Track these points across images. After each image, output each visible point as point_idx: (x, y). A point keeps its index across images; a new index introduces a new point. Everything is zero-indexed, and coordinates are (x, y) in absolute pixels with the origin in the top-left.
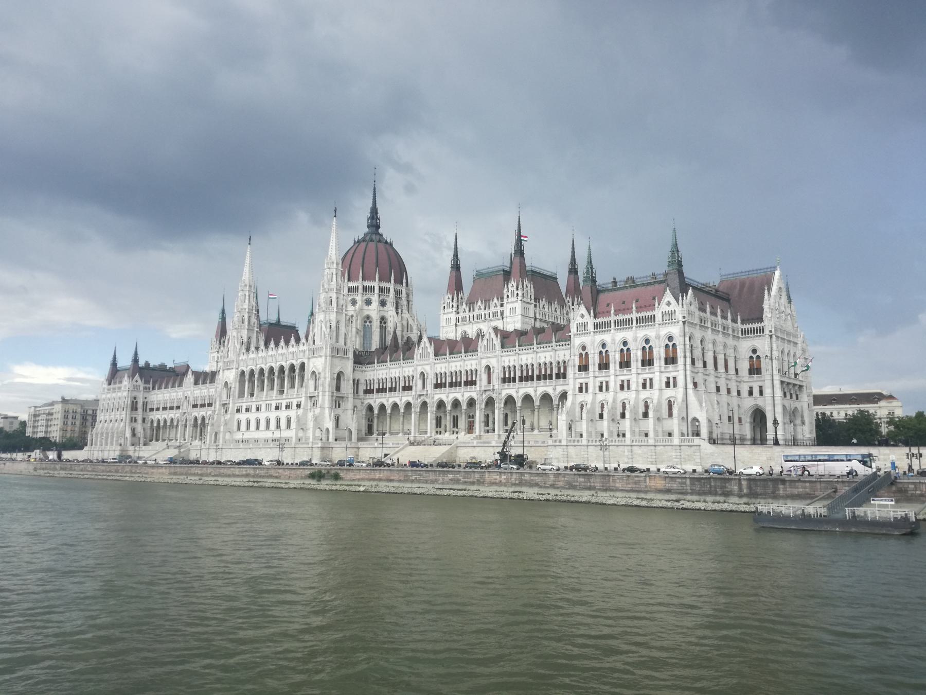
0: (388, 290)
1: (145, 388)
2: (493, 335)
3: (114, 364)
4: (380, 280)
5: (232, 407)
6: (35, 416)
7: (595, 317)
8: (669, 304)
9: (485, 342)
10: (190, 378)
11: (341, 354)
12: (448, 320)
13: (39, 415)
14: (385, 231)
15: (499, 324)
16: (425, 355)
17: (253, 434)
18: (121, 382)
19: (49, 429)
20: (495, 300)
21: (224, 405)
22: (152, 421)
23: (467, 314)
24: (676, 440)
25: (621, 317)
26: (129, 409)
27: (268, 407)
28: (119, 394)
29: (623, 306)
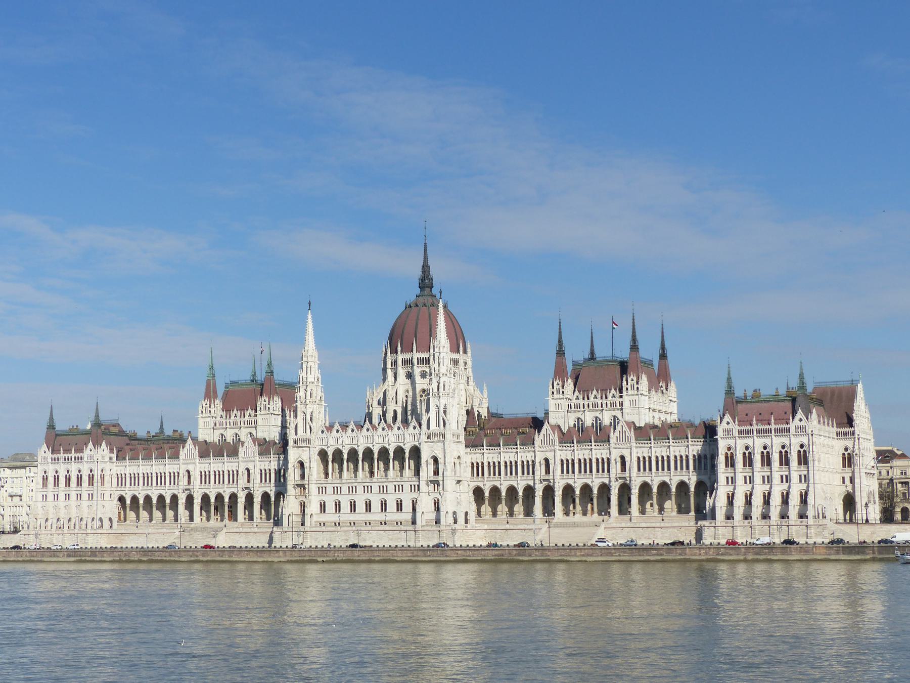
1: (111, 458)
2: (626, 428)
3: (51, 426)
5: (313, 488)
8: (801, 420)
9: (617, 433)
12: (558, 406)
15: (618, 414)
16: (547, 442)
18: (81, 451)
20: (613, 391)
23: (581, 402)
24: (811, 521)
25: (761, 427)
26: (99, 484)
27: (368, 489)
29: (760, 417)
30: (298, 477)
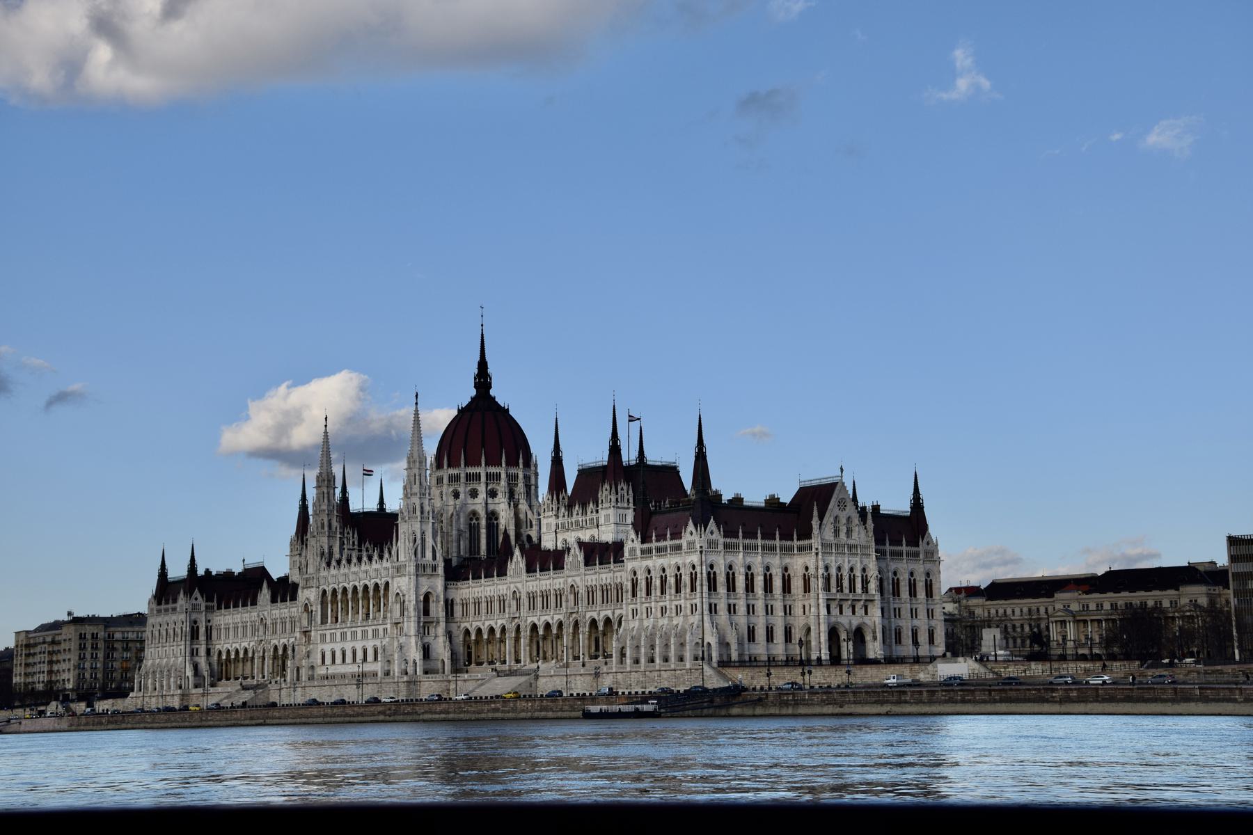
0: (497, 477)
4: (486, 464)
6: (28, 646)
7: (643, 542)
10: (265, 594)
11: (429, 571)
12: (549, 525)
13: (35, 645)
14: (499, 393)
17: (339, 669)
18: (175, 601)
19: (55, 668)
21: (305, 632)
22: (220, 653)
26: (188, 638)
28: (174, 617)
30: (305, 623)
